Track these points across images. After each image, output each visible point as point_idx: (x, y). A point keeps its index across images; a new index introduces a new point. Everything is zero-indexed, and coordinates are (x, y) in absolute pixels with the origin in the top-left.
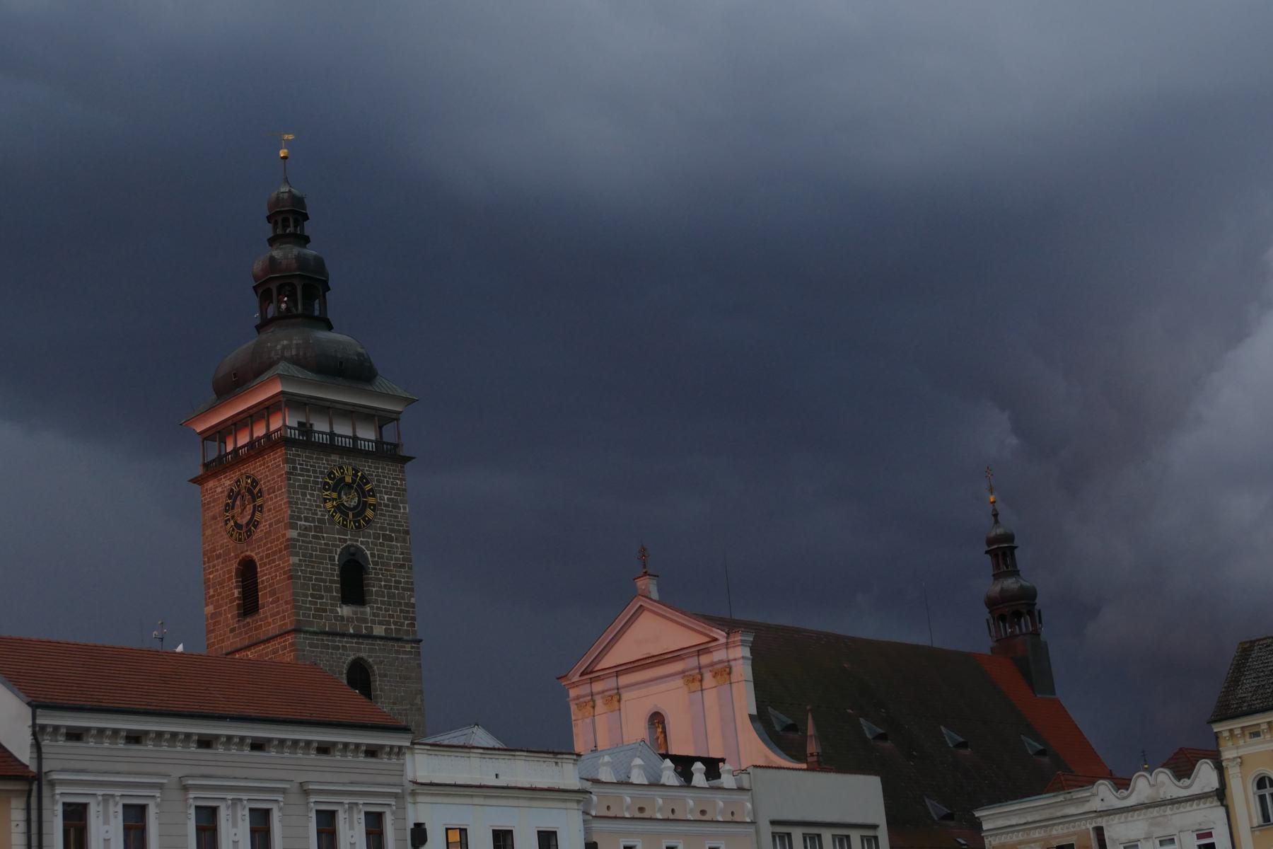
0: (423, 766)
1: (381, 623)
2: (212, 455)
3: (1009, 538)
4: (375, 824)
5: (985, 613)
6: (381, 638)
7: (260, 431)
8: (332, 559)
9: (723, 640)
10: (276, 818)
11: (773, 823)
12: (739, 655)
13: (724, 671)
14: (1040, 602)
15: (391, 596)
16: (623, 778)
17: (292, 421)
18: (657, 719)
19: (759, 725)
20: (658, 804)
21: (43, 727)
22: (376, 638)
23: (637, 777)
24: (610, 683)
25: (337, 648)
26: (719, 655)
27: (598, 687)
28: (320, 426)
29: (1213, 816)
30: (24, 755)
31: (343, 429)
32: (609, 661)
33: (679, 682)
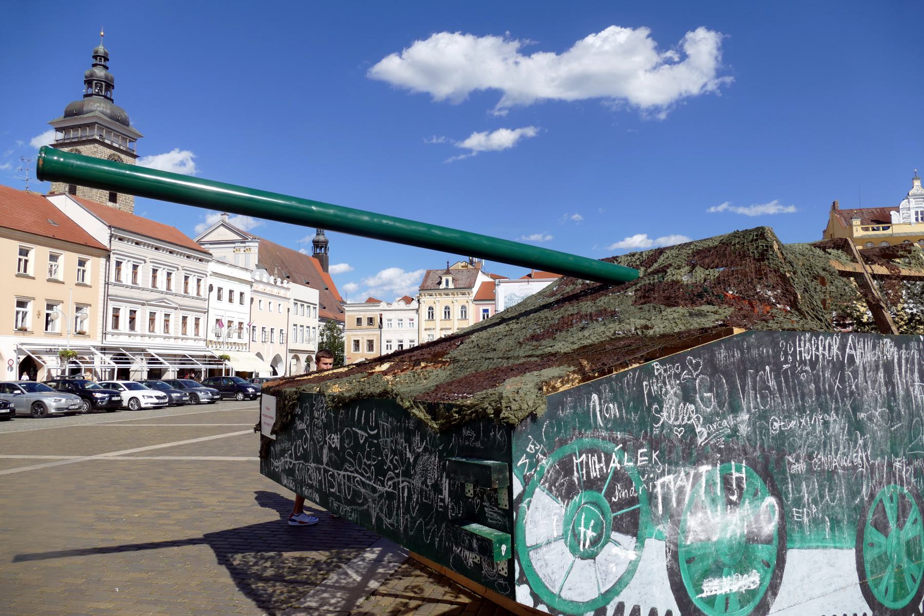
5: (312, 245)
12: (254, 246)
20: (268, 289)
23: (265, 280)
29: (413, 315)
33: (232, 250)
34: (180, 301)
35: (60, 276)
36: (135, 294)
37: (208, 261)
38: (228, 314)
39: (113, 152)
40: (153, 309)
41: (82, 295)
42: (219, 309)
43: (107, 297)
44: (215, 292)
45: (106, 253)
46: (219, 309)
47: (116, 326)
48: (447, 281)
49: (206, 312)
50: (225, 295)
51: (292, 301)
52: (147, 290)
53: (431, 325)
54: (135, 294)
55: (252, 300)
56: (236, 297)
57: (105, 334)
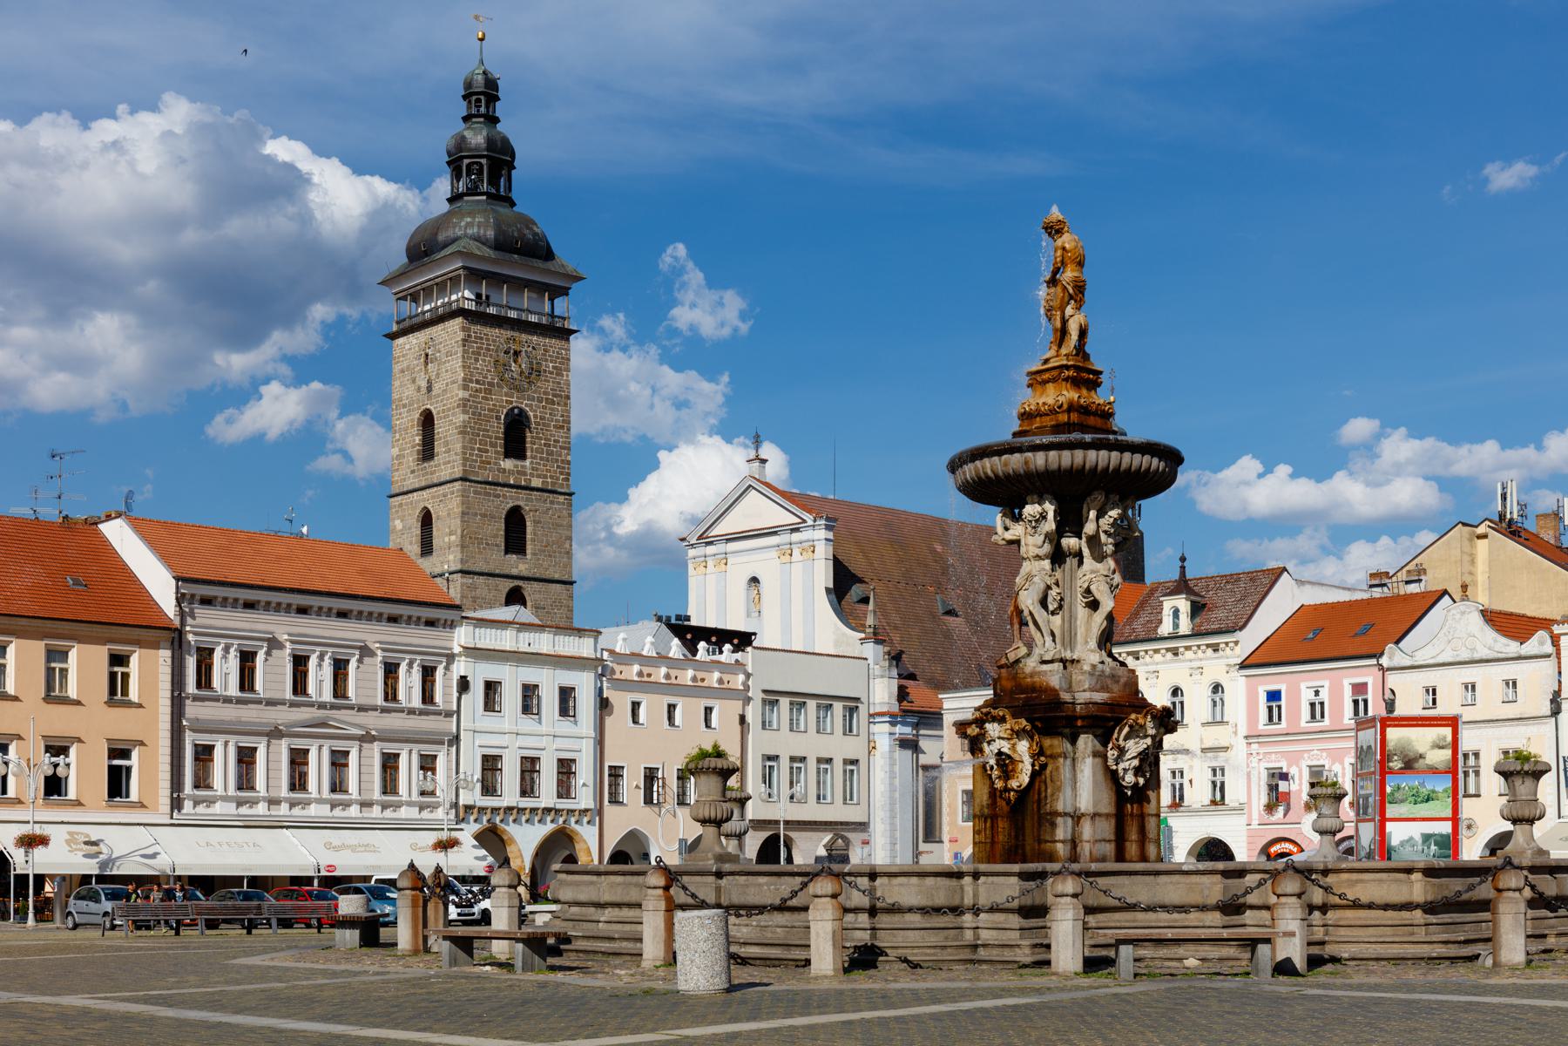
1: (539, 476)
4: (428, 673)
6: (538, 490)
8: (498, 418)
9: (810, 522)
11: (765, 691)
15: (552, 453)
16: (636, 651)
19: (833, 597)
21: (183, 595)
22: (533, 489)
23: (648, 650)
25: (498, 496)
27: (711, 550)
32: (719, 530)
33: (774, 553)
35: (72, 692)
36: (250, 714)
37: (452, 625)
38: (521, 741)
39: (509, 333)
41: (121, 724)
42: (483, 731)
44: (478, 690)
46: (483, 731)
47: (202, 781)
48: (1176, 613)
49: (456, 740)
50: (511, 697)
51: (756, 694)
52: (282, 702)
54: (250, 714)
55: (604, 705)
56: (549, 700)
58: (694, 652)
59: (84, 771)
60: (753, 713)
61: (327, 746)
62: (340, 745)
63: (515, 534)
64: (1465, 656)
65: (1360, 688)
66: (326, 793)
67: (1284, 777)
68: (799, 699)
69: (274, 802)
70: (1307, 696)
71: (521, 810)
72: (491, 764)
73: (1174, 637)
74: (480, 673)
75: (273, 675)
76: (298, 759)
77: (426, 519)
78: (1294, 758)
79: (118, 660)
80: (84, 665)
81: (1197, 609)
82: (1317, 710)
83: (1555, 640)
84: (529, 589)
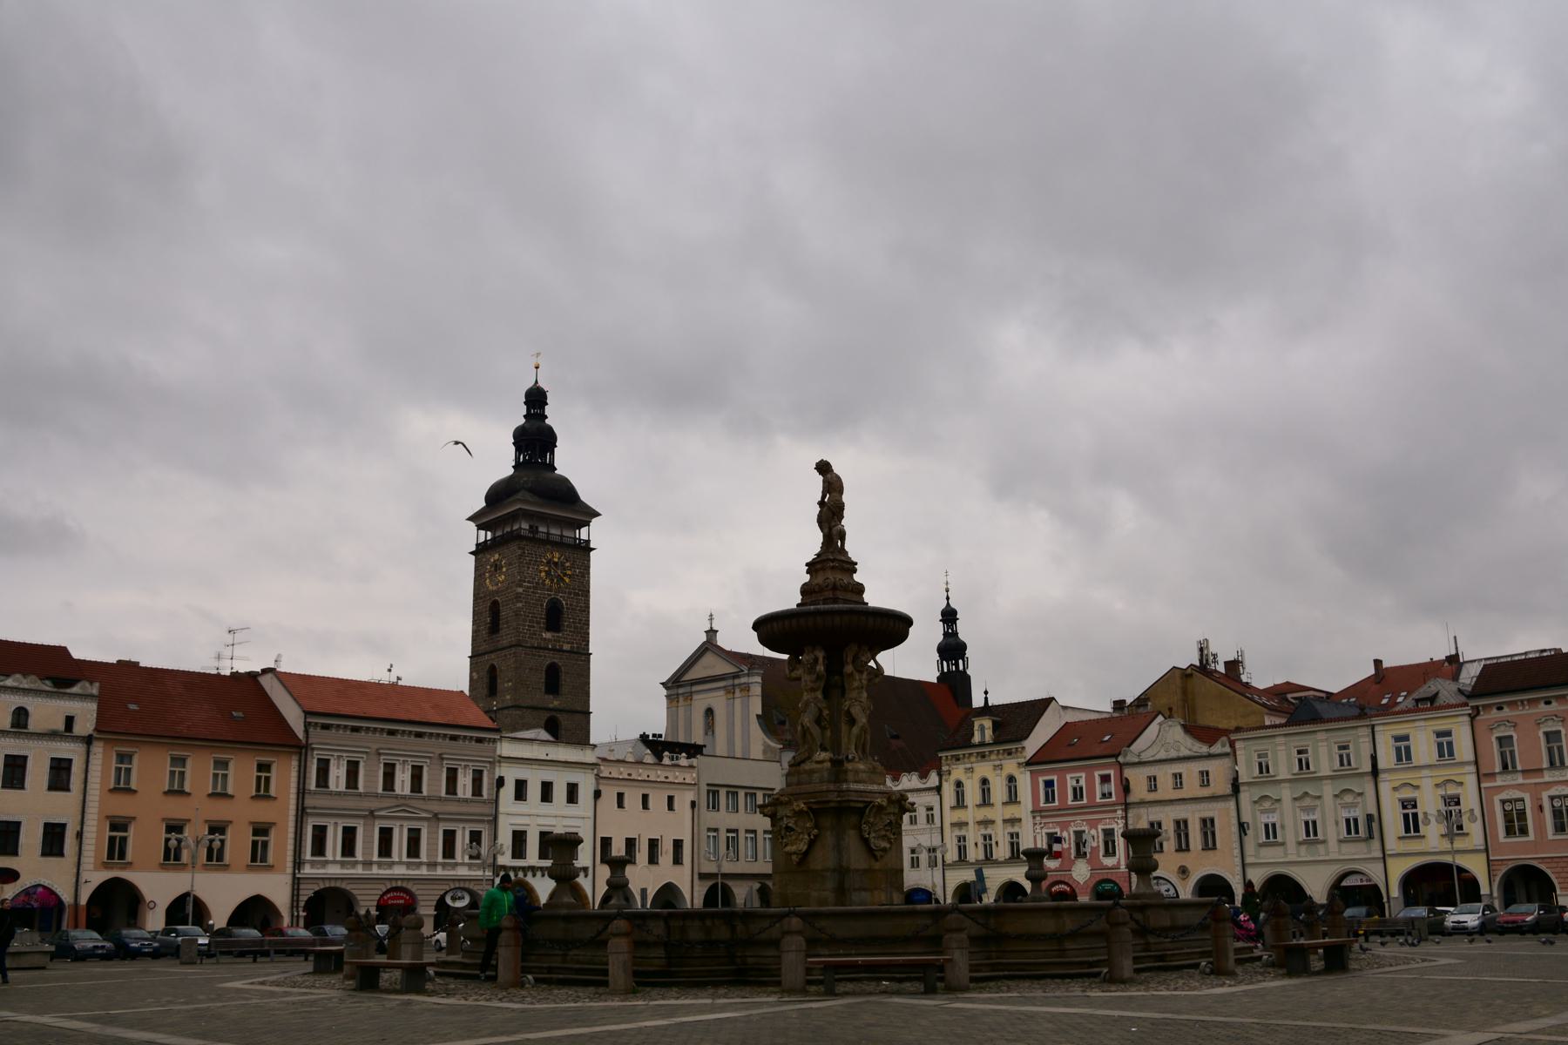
0: (506, 749)
2: (482, 539)
3: (954, 612)
7: (508, 529)
10: (425, 770)
13: (746, 688)
14: (968, 653)
17: (525, 526)
18: (709, 712)
20: (642, 773)
24: (688, 689)
26: (743, 680)
27: (681, 691)
28: (542, 529)
29: (932, 799)
30: (301, 735)
31: (555, 531)
32: (687, 677)
33: (722, 693)
34: (436, 807)
37: (494, 741)
38: (541, 821)
40: (386, 824)
41: (263, 812)
43: (302, 813)
45: (300, 749)
46: (513, 815)
47: (319, 847)
48: (982, 728)
50: (534, 791)
53: (960, 815)
54: (350, 803)
55: (597, 794)
56: (560, 792)
57: (298, 863)
58: (660, 758)
59: (237, 843)
60: (703, 803)
61: (407, 825)
62: (415, 825)
63: (553, 680)
64: (1173, 754)
65: (1105, 779)
66: (405, 859)
67: (1059, 840)
68: (733, 791)
69: (368, 864)
70: (1071, 783)
71: (541, 869)
72: (519, 838)
73: (982, 744)
74: (511, 774)
75: (371, 778)
76: (386, 836)
77: (493, 673)
78: (1064, 826)
79: (264, 767)
80: (241, 772)
81: (996, 726)
82: (1078, 794)
83: (1232, 744)
84: (561, 717)
